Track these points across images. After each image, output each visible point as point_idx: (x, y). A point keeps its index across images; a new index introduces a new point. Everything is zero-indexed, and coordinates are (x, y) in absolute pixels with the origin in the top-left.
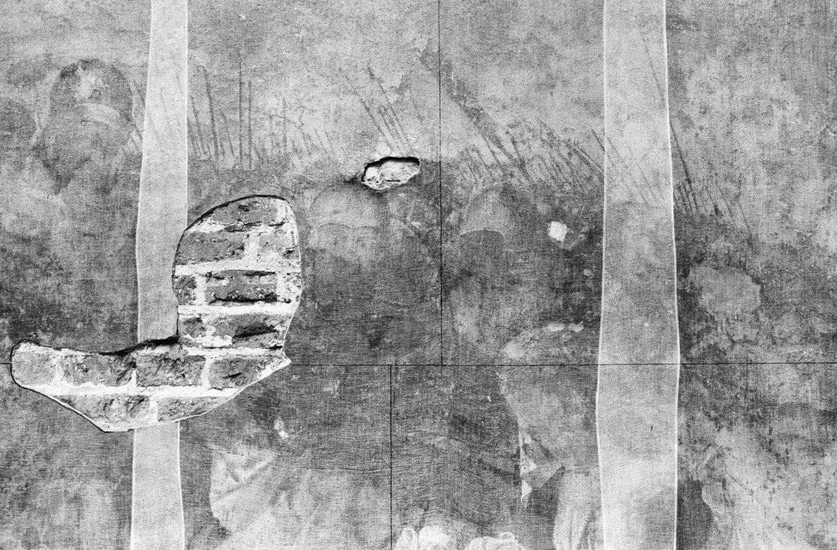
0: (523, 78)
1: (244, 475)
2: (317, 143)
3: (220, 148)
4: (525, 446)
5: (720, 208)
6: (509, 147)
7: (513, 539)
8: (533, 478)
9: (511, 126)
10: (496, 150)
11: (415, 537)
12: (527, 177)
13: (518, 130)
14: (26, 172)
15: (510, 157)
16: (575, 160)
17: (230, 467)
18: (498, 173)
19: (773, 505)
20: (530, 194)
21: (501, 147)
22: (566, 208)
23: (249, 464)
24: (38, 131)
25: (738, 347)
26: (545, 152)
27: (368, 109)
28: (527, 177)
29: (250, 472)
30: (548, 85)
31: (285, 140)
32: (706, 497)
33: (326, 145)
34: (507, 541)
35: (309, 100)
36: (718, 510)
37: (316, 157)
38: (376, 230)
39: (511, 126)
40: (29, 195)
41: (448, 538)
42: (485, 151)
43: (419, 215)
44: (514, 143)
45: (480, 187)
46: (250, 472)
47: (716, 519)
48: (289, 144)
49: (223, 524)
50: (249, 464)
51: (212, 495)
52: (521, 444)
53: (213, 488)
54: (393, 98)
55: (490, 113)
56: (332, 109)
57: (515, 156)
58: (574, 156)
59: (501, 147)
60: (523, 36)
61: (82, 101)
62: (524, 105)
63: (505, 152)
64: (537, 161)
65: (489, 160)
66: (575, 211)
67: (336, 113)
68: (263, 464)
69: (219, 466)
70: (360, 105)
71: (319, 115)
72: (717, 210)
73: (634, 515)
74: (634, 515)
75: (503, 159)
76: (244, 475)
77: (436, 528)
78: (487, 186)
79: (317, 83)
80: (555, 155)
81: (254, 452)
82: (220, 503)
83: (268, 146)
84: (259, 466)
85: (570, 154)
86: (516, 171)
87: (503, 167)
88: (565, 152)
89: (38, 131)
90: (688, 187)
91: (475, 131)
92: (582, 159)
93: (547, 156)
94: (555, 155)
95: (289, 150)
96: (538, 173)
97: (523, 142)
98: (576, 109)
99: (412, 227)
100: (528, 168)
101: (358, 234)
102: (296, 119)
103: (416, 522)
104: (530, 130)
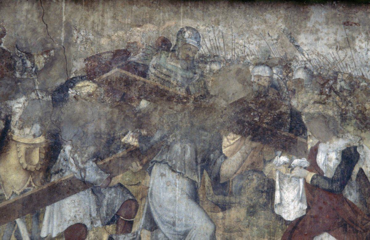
0: (311, 38)
1: (232, 142)
2: (253, 53)
3: (226, 54)
4: (309, 135)
6: (306, 56)
7: (306, 160)
9: (307, 51)
10: (303, 57)
11: (279, 159)
12: (311, 64)
13: (309, 52)
14: (169, 58)
15: (307, 59)
16: (324, 60)
17: (228, 140)
18: (303, 63)
20: (312, 69)
21: (304, 56)
22: (321, 73)
23: (234, 139)
24: (173, 46)
25: (367, 111)
26: (316, 58)
27: (268, 45)
28: (311, 64)
29: (234, 141)
30: (317, 39)
31: (245, 52)
32: (358, 150)
33: (256, 53)
34: (304, 160)
35: (252, 41)
36: (361, 153)
37: (253, 57)
38: (269, 77)
39: (307, 51)
40: (170, 64)
41: (288, 159)
42: (300, 57)
43: (281, 73)
44: (308, 55)
45: (298, 66)
46: (234, 141)
47: (361, 156)
48: (246, 53)
49: (226, 155)
50: (234, 139)
51: (223, 147)
52: (308, 135)
53: (223, 146)
54: (275, 41)
55: (302, 47)
56: (258, 44)
59: (304, 56)
60: (311, 26)
61: (186, 38)
62: (311, 45)
63: (305, 57)
64: (314, 60)
65: (301, 59)
66: (324, 74)
67: (259, 45)
68: (237, 139)
69: (225, 139)
70: (265, 43)
71: (254, 45)
72: (363, 75)
73: (339, 154)
74: (339, 154)
75: (305, 59)
76: (232, 142)
77: (285, 157)
78: (300, 67)
79: (254, 37)
80: (319, 58)
81: (235, 136)
82: (225, 149)
83: (240, 53)
84: (236, 140)
85: (323, 59)
86: (308, 63)
87: (305, 61)
88: (322, 58)
89: (173, 46)
90: (355, 68)
91: (297, 51)
92: (326, 60)
93: (317, 59)
94: (319, 58)
95: (246, 54)
96: (314, 63)
97: (310, 55)
98: (325, 46)
99: (280, 77)
100: (311, 62)
101: (265, 78)
102: (248, 46)
103: (279, 155)
104: (312, 52)
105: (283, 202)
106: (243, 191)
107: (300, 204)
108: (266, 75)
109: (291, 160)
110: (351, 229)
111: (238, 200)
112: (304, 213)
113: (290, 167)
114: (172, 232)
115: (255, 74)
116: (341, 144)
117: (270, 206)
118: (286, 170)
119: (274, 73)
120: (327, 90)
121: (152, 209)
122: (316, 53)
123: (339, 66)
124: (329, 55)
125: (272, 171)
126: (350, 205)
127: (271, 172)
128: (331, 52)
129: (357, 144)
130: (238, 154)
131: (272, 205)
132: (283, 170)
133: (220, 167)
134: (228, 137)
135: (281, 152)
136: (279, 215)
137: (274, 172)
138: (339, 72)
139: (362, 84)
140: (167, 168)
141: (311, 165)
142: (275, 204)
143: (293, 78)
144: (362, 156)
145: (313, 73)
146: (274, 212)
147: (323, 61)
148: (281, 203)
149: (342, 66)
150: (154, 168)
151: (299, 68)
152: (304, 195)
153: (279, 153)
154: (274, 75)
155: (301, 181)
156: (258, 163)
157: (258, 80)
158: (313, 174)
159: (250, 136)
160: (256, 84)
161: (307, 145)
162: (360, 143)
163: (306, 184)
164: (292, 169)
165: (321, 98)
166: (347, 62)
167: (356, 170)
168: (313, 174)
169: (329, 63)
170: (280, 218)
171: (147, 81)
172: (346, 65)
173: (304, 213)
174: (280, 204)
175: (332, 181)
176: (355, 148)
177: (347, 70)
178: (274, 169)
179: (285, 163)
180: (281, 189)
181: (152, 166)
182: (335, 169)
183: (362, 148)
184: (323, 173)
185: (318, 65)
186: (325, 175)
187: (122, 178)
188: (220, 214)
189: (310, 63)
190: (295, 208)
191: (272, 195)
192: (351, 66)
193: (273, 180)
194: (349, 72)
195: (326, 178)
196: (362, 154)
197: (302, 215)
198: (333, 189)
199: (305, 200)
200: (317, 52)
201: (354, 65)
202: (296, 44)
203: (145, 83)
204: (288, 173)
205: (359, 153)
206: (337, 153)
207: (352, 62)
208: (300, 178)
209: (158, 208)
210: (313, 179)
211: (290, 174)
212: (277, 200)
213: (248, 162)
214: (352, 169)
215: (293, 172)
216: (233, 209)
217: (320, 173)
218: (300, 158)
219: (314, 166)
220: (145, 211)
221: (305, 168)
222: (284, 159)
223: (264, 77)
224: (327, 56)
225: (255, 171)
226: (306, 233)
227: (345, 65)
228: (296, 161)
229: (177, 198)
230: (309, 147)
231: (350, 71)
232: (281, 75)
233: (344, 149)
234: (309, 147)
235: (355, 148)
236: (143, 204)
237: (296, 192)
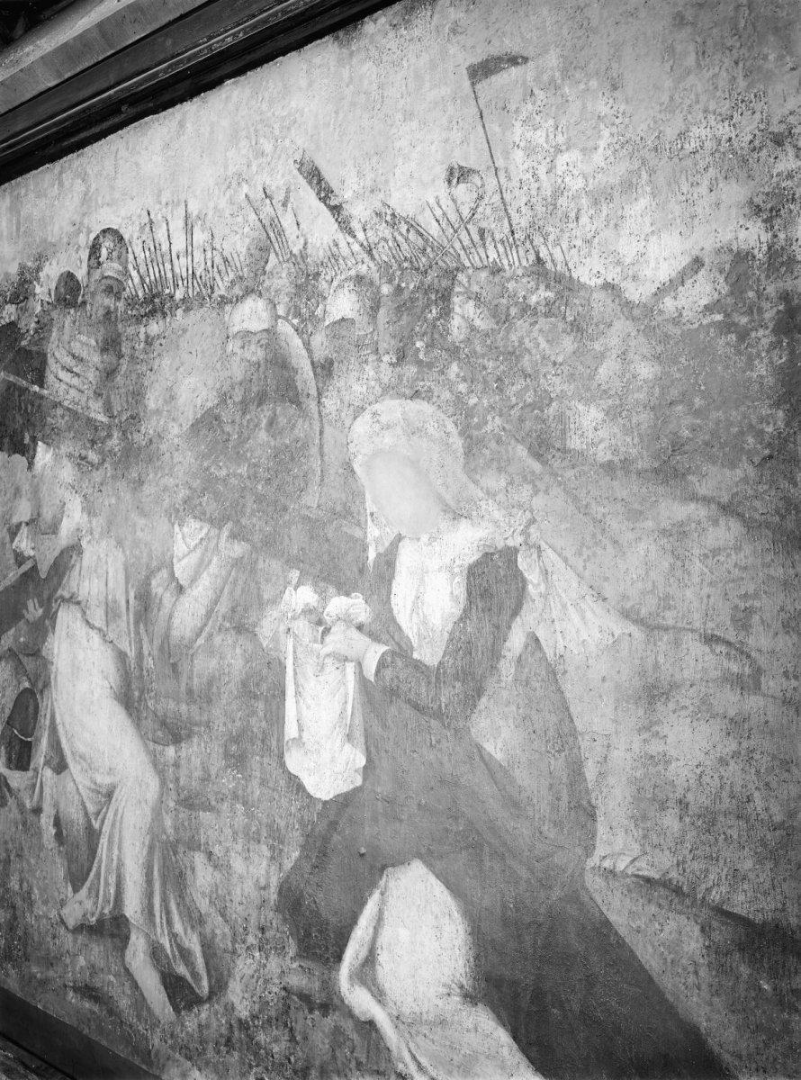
5: (541, 255)
8: (377, 541)
10: (351, 240)
19: (587, 574)
21: (355, 237)
32: (522, 563)
34: (356, 601)
36: (533, 577)
42: (343, 244)
52: (368, 512)
57: (365, 243)
58: (412, 231)
64: (383, 243)
74: (457, 580)
78: (343, 277)
80: (396, 234)
85: (408, 230)
88: (404, 228)
100: (374, 252)
103: (294, 581)
105: (305, 735)
106: (214, 689)
107: (348, 747)
108: (260, 329)
109: (324, 599)
110: (497, 867)
111: (205, 718)
112: (359, 782)
113: (320, 622)
114: (88, 783)
115: (236, 329)
116: (465, 542)
117: (274, 743)
118: (311, 631)
119: (279, 317)
120: (419, 344)
121: (58, 720)
122: (389, 218)
123: (457, 245)
124: (428, 212)
125: (276, 632)
126: (492, 775)
127: (275, 639)
128: (432, 201)
129: (516, 541)
130: (205, 581)
131: (278, 740)
132: (302, 627)
133: (170, 618)
134: (185, 529)
135: (297, 573)
136: (296, 777)
137: (282, 637)
138: (457, 269)
139: (533, 299)
140: (79, 615)
141: (377, 617)
142: (286, 739)
143: (327, 323)
144: (534, 585)
145: (379, 288)
146: (283, 765)
147: (407, 239)
148: (301, 737)
149: (467, 242)
150: (59, 614)
151: (340, 286)
152: (358, 720)
153: (294, 575)
154: (280, 321)
155: (350, 668)
156: (246, 610)
157: (243, 347)
158: (383, 648)
159: (229, 525)
160: (238, 359)
161: (365, 550)
162: (529, 535)
163: (362, 680)
164: (327, 631)
165: (400, 377)
166: (484, 225)
167: (516, 641)
168: (383, 648)
169: (426, 241)
170: (296, 785)
171: (45, 392)
172: (482, 232)
173: (359, 782)
174: (298, 741)
175: (436, 676)
176: (510, 555)
177: (484, 256)
178: (282, 628)
179: (308, 611)
180: (298, 693)
181: (57, 610)
182: (446, 636)
183: (535, 556)
184: (412, 648)
185: (394, 257)
186: (416, 656)
187: (16, 639)
188: (171, 751)
189: (373, 258)
190: (333, 760)
191: (278, 708)
192: (498, 237)
193: (280, 663)
194: (491, 260)
195: (418, 666)
196: (536, 582)
197: (351, 787)
198: (440, 706)
199: (359, 734)
200: (389, 212)
201: (507, 230)
202: (333, 203)
203: (42, 397)
204: (315, 641)
205: (526, 575)
206: (453, 575)
207: (500, 219)
208: (346, 659)
209: (67, 719)
210: (382, 665)
211: (320, 646)
212: (291, 730)
213: (223, 608)
214: (500, 633)
215: (328, 639)
216: (195, 740)
217: (400, 652)
218: (347, 594)
219: (383, 627)
220: (48, 723)
221: (360, 628)
222: (305, 595)
223: (255, 334)
224: (420, 219)
225: (240, 629)
226: (363, 850)
227: (476, 238)
228: (337, 604)
229: (96, 695)
230: (372, 555)
231: (493, 255)
232: (295, 317)
233: (475, 558)
234: (372, 555)
235: (510, 555)
236: (45, 704)
237: (338, 709)
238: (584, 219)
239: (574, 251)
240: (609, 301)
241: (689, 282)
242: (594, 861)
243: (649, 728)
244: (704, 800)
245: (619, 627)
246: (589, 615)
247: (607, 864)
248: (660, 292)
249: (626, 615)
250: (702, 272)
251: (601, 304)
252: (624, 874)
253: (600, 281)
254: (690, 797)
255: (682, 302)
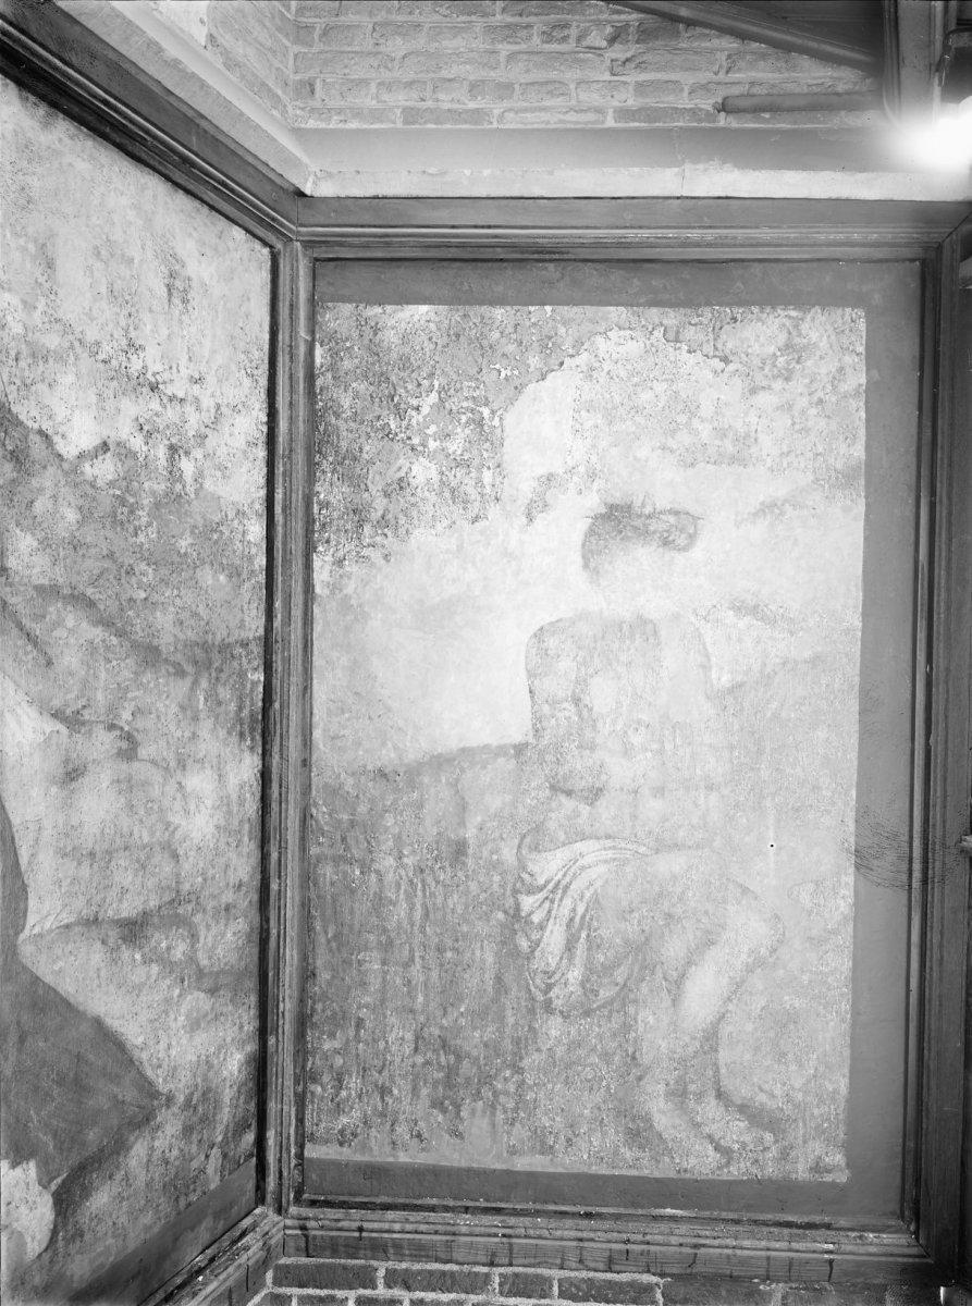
238: (22, 364)
239: (13, 388)
240: (44, 447)
241: (100, 458)
242: (22, 937)
243: (67, 804)
244: (106, 846)
245: (51, 726)
246: (24, 718)
247: (36, 931)
248: (81, 456)
249: (57, 715)
250: (109, 454)
251: (37, 448)
252: (51, 931)
253: (36, 426)
254: (97, 848)
255: (96, 471)
